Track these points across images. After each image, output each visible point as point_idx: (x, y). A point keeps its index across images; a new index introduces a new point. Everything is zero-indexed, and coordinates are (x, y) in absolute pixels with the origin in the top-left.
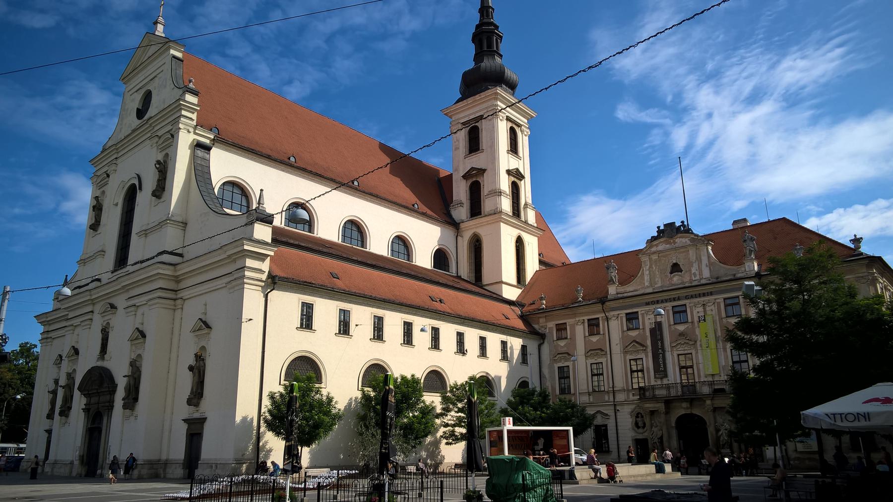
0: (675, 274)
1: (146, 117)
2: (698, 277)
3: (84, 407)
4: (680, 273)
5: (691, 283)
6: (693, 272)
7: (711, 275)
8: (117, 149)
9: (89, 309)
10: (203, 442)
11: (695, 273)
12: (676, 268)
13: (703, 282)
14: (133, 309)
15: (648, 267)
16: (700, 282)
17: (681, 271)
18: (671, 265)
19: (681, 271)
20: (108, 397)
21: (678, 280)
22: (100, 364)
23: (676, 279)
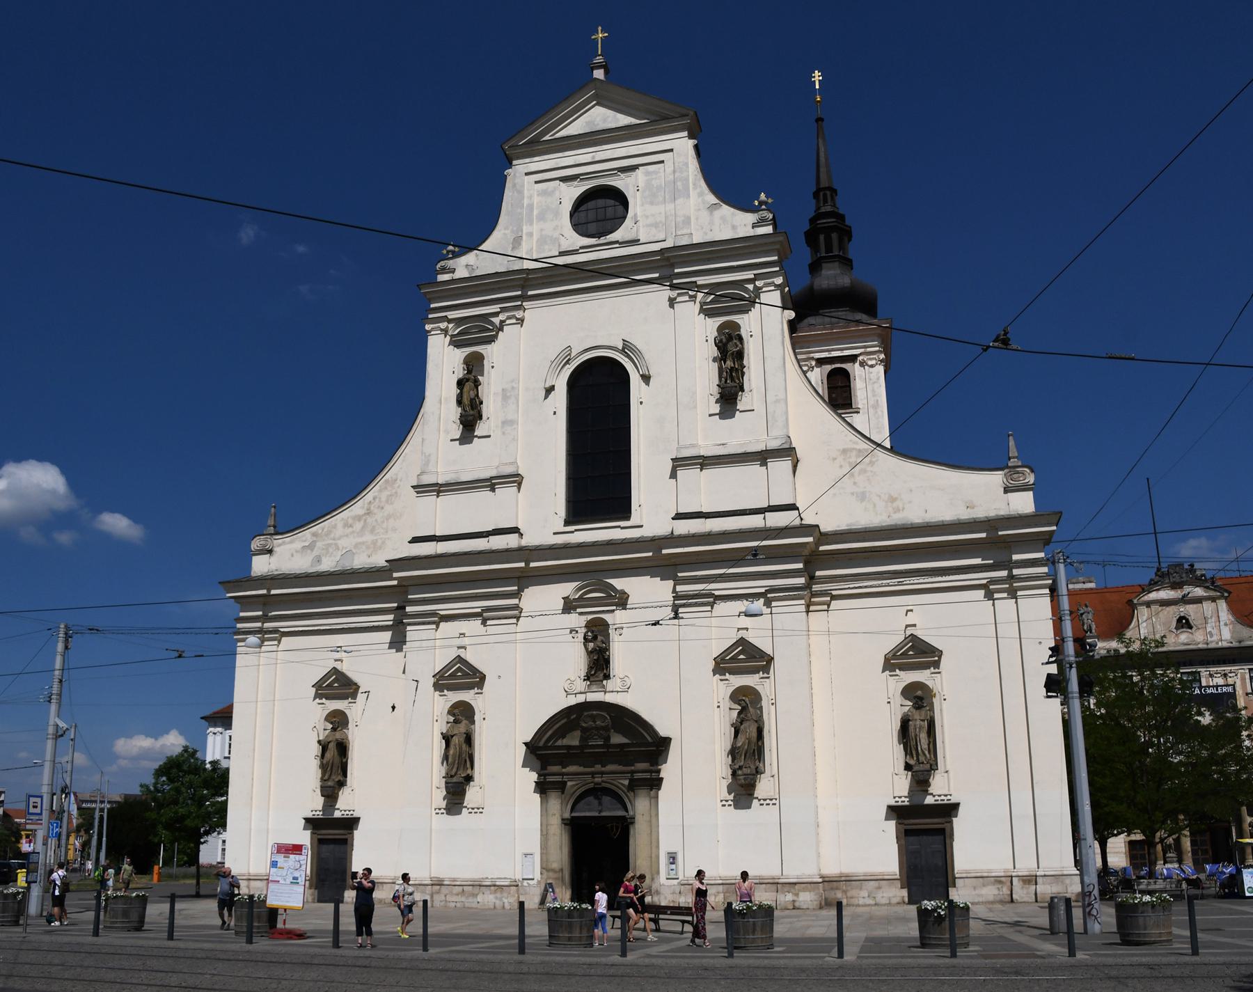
0: (1184, 630)
1: (616, 236)
2: (1215, 638)
4: (1190, 631)
5: (1207, 644)
6: (1208, 631)
7: (1232, 637)
8: (526, 280)
10: (955, 844)
11: (1210, 632)
12: (1184, 623)
13: (1225, 644)
15: (1145, 618)
16: (1217, 643)
17: (1191, 627)
18: (1177, 617)
19: (1191, 627)
21: (1188, 638)
23: (1184, 637)
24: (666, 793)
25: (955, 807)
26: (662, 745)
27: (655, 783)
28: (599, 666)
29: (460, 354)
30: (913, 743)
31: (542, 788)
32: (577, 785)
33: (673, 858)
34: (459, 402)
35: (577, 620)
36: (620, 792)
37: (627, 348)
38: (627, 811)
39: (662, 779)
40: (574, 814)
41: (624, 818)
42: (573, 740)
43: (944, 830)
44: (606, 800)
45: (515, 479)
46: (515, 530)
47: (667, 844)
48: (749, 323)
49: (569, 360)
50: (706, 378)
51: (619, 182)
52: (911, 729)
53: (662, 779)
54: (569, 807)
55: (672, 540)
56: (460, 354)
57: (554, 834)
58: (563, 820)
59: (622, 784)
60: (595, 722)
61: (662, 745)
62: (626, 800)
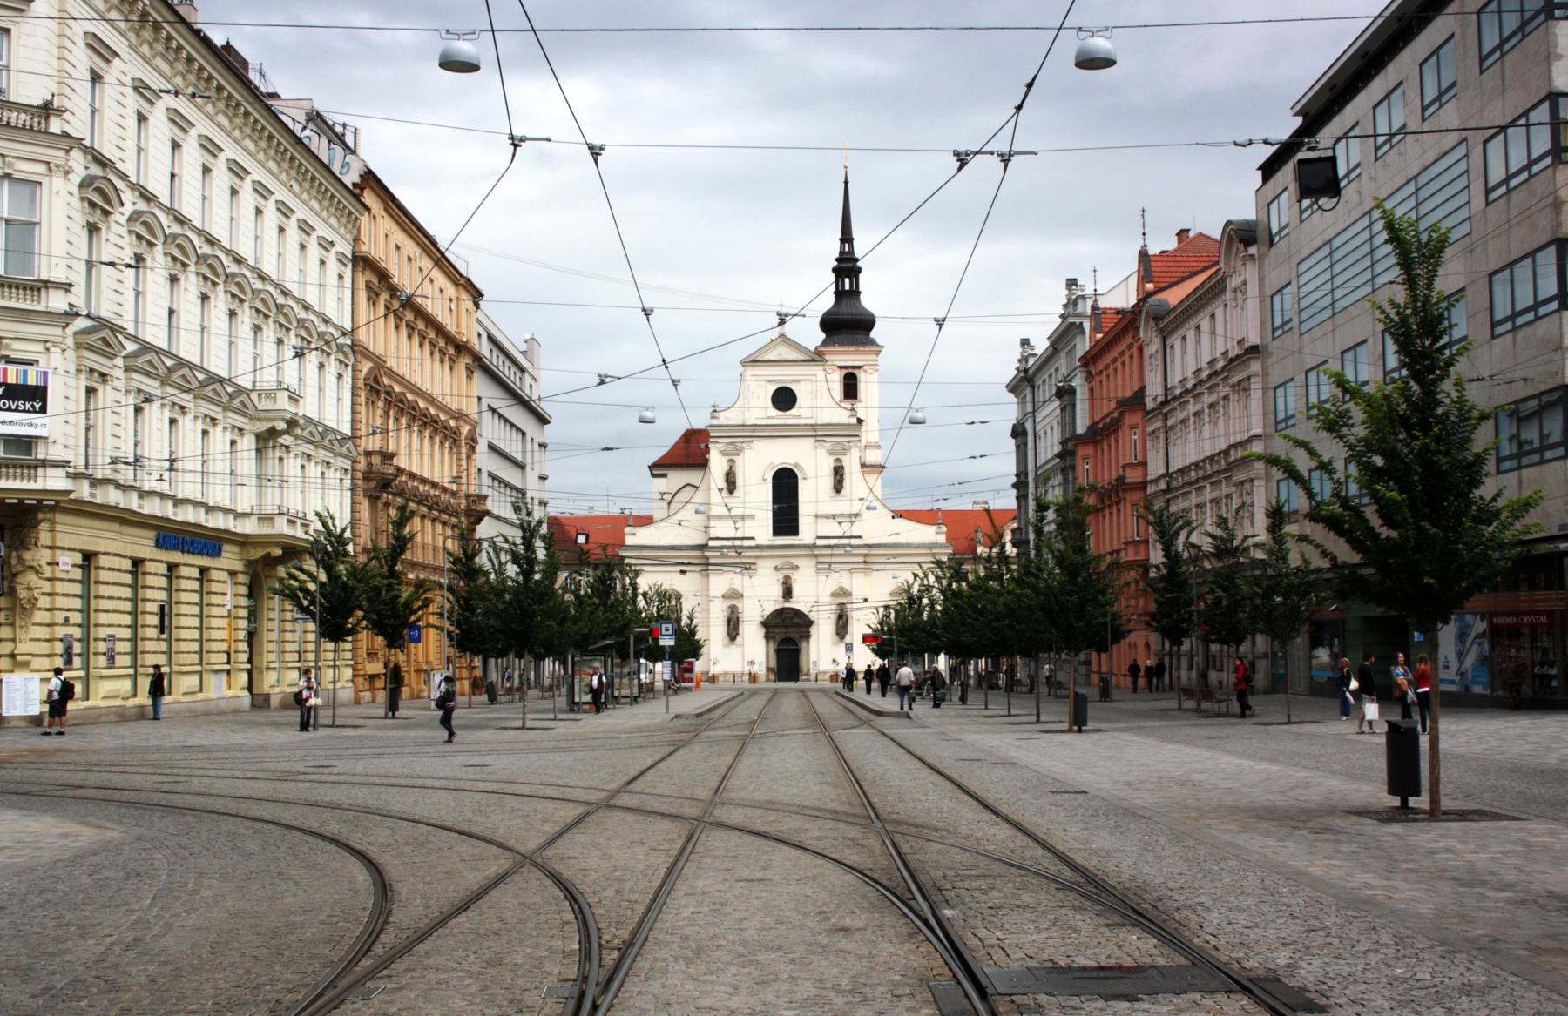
1: (792, 412)
22: (787, 605)
24: (812, 640)
26: (811, 623)
27: (808, 636)
28: (788, 593)
29: (725, 459)
31: (767, 637)
33: (815, 663)
35: (780, 576)
37: (797, 465)
42: (778, 621)
45: (752, 517)
46: (753, 538)
47: (813, 657)
48: (846, 462)
50: (828, 481)
51: (793, 387)
55: (814, 546)
56: (725, 459)
61: (811, 623)
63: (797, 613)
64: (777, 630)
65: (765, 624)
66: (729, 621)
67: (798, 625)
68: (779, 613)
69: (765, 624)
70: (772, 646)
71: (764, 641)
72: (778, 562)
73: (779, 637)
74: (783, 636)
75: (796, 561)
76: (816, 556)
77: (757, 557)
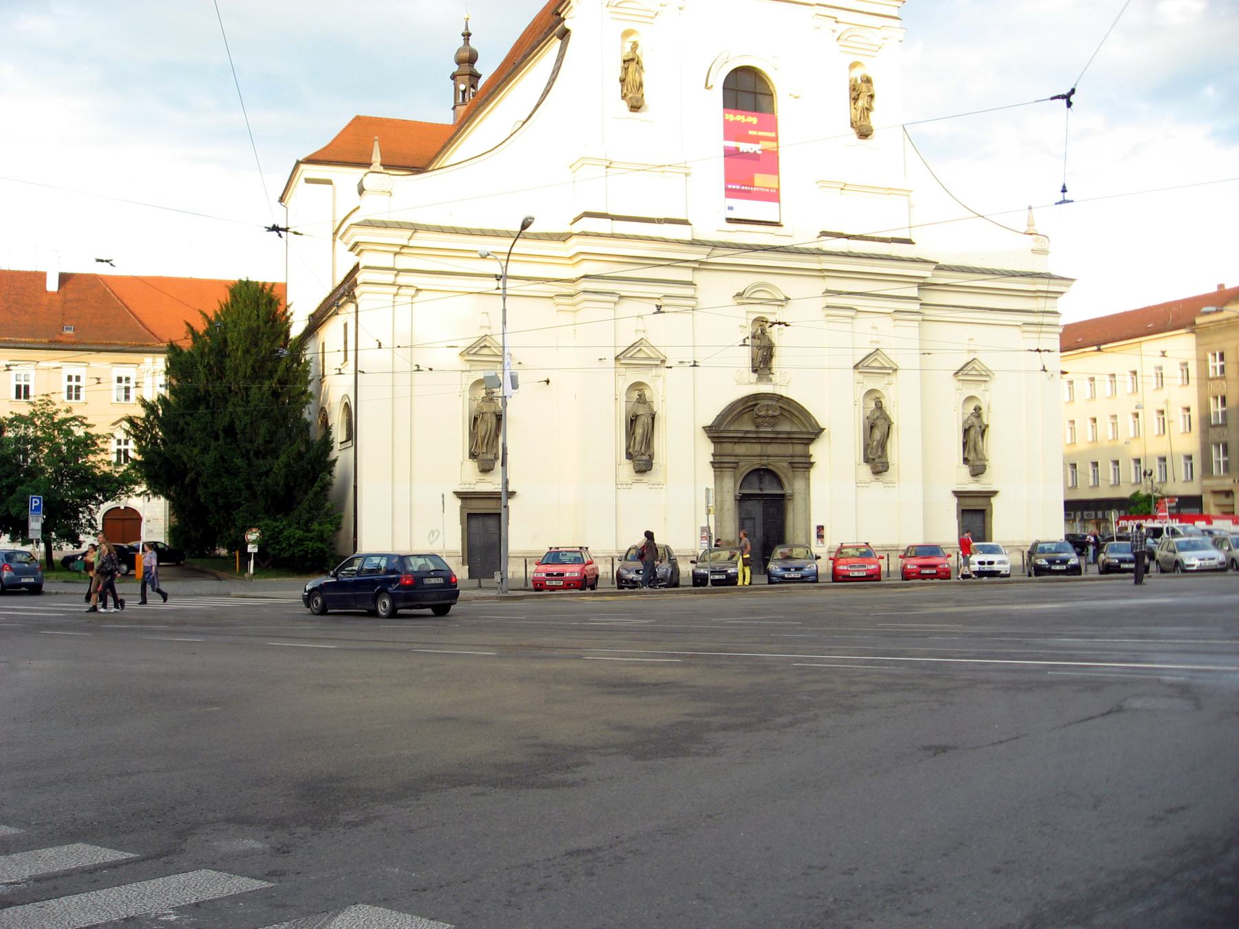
3: (711, 459)
9: (686, 275)
14: (851, 313)
20: (799, 449)
24: (814, 473)
25: (995, 493)
26: (815, 433)
27: (809, 465)
28: (763, 360)
30: (971, 444)
31: (718, 465)
32: (746, 465)
34: (622, 81)
36: (780, 473)
38: (782, 487)
39: (813, 463)
40: (743, 492)
41: (783, 496)
43: (982, 512)
44: (767, 479)
46: (685, 222)
49: (726, 62)
52: (972, 432)
53: (813, 463)
54: (738, 486)
57: (729, 509)
58: (735, 496)
59: (783, 467)
60: (767, 410)
62: (784, 480)
63: (787, 408)
64: (741, 449)
65: (716, 433)
66: (632, 421)
67: (789, 439)
68: (748, 406)
69: (716, 433)
70: (730, 487)
71: (710, 473)
72: (742, 282)
73: (745, 468)
74: (756, 463)
75: (785, 286)
76: (823, 273)
77: (701, 265)
